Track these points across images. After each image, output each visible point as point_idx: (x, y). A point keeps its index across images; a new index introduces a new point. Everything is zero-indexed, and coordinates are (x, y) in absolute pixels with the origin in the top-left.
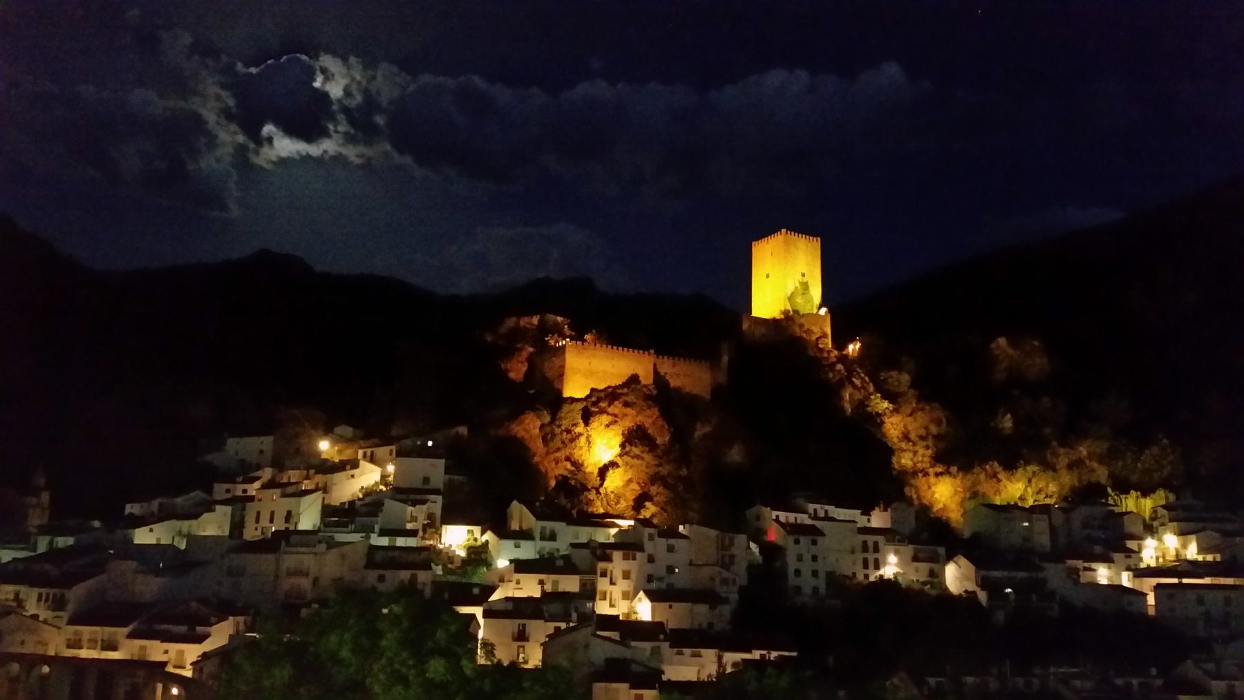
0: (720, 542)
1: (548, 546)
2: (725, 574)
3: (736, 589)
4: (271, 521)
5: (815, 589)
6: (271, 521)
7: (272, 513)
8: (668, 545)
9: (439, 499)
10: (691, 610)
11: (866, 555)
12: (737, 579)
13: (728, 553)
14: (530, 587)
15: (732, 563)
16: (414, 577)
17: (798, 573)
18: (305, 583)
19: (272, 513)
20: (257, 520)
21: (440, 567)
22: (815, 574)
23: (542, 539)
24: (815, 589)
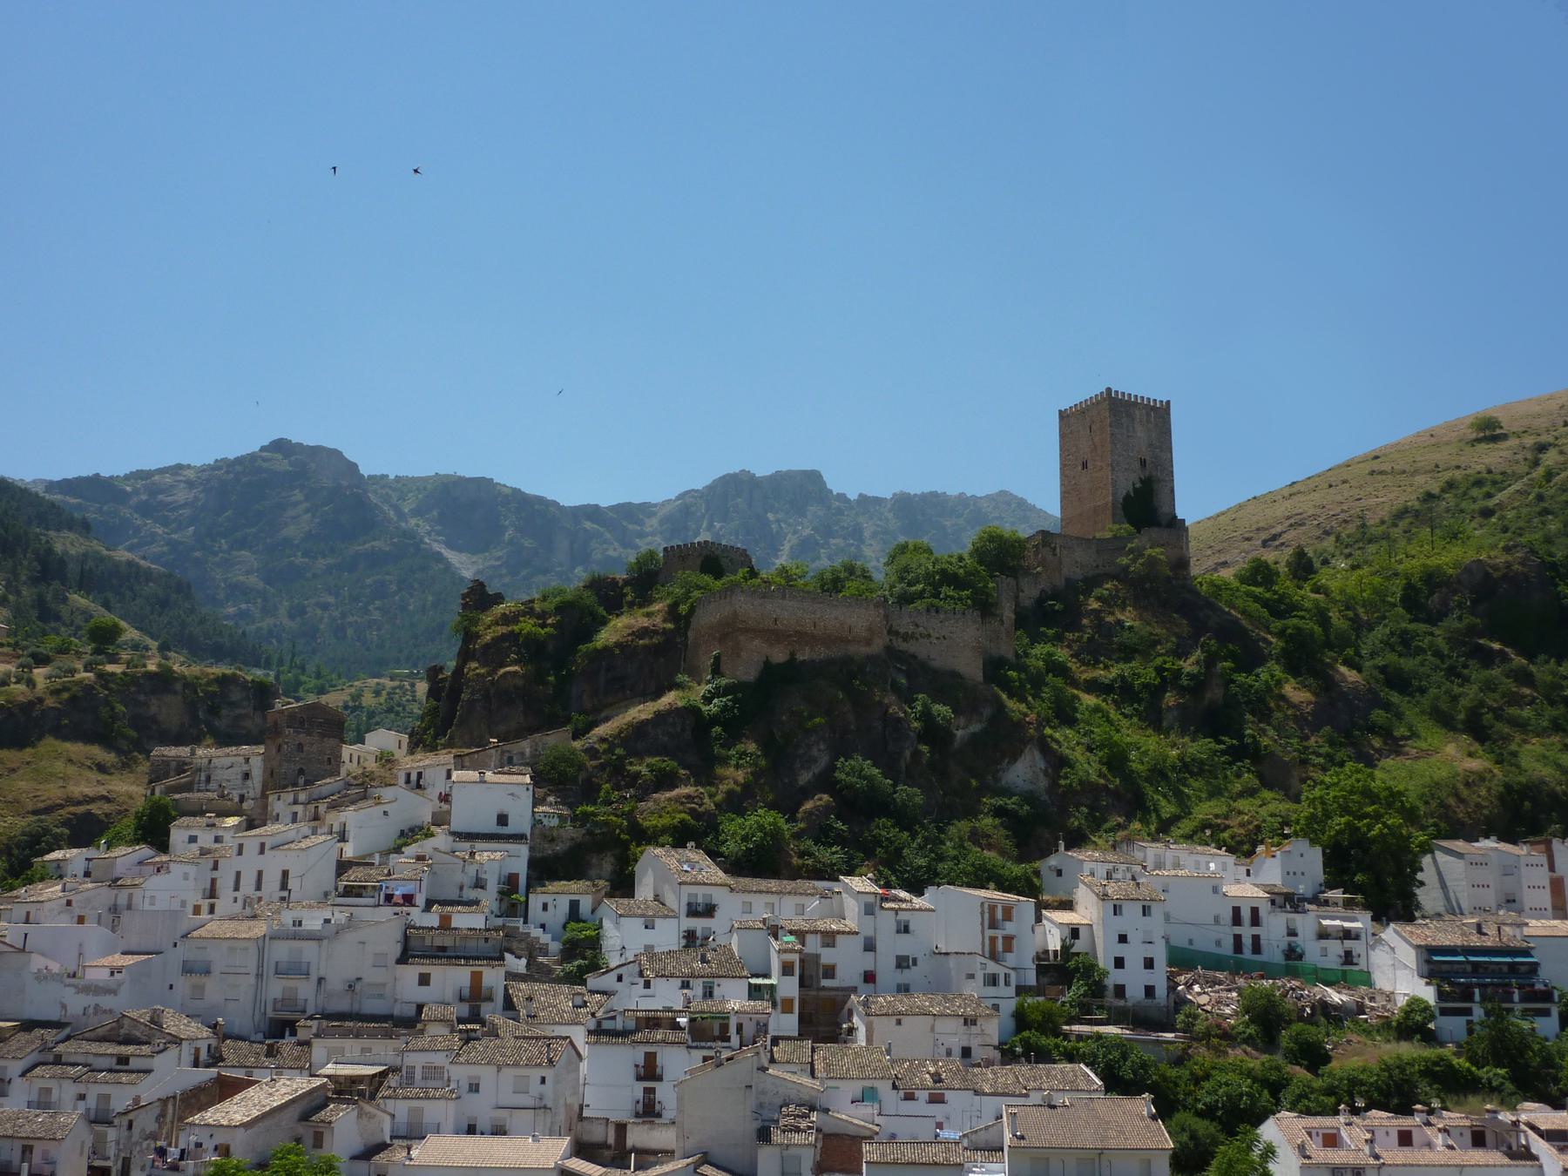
0: (987, 916)
1: (699, 924)
2: (992, 967)
3: (1011, 991)
4: (258, 888)
5: (1150, 991)
6: (258, 888)
7: (260, 873)
8: (898, 922)
9: (523, 851)
10: (932, 1029)
11: (1237, 930)
12: (1013, 975)
13: (999, 933)
14: (666, 996)
15: (1008, 948)
16: (476, 978)
17: (1119, 963)
18: (305, 991)
19: (260, 873)
20: (237, 889)
21: (524, 961)
22: (1149, 964)
23: (693, 912)
24: (1150, 991)
